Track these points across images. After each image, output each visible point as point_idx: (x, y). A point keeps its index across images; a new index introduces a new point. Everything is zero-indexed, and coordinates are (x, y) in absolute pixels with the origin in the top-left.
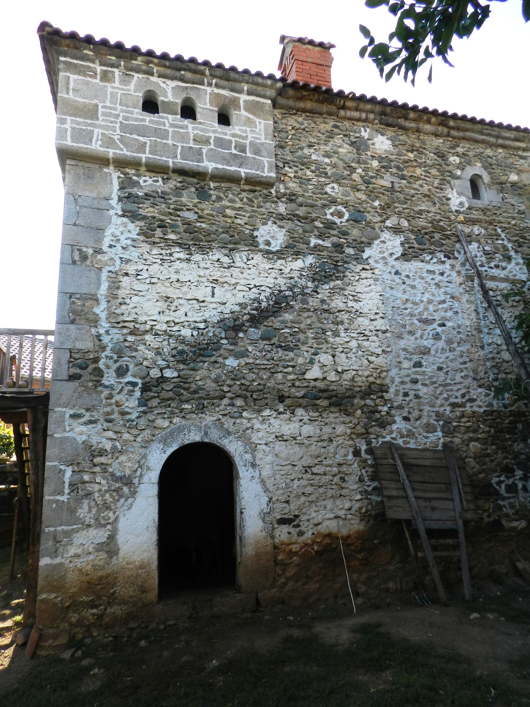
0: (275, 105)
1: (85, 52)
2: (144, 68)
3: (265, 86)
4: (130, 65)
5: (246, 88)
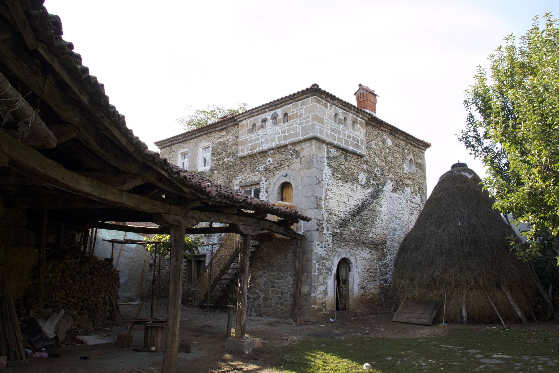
0: (367, 123)
1: (323, 95)
2: (337, 104)
3: (366, 116)
4: (333, 103)
5: (361, 116)
